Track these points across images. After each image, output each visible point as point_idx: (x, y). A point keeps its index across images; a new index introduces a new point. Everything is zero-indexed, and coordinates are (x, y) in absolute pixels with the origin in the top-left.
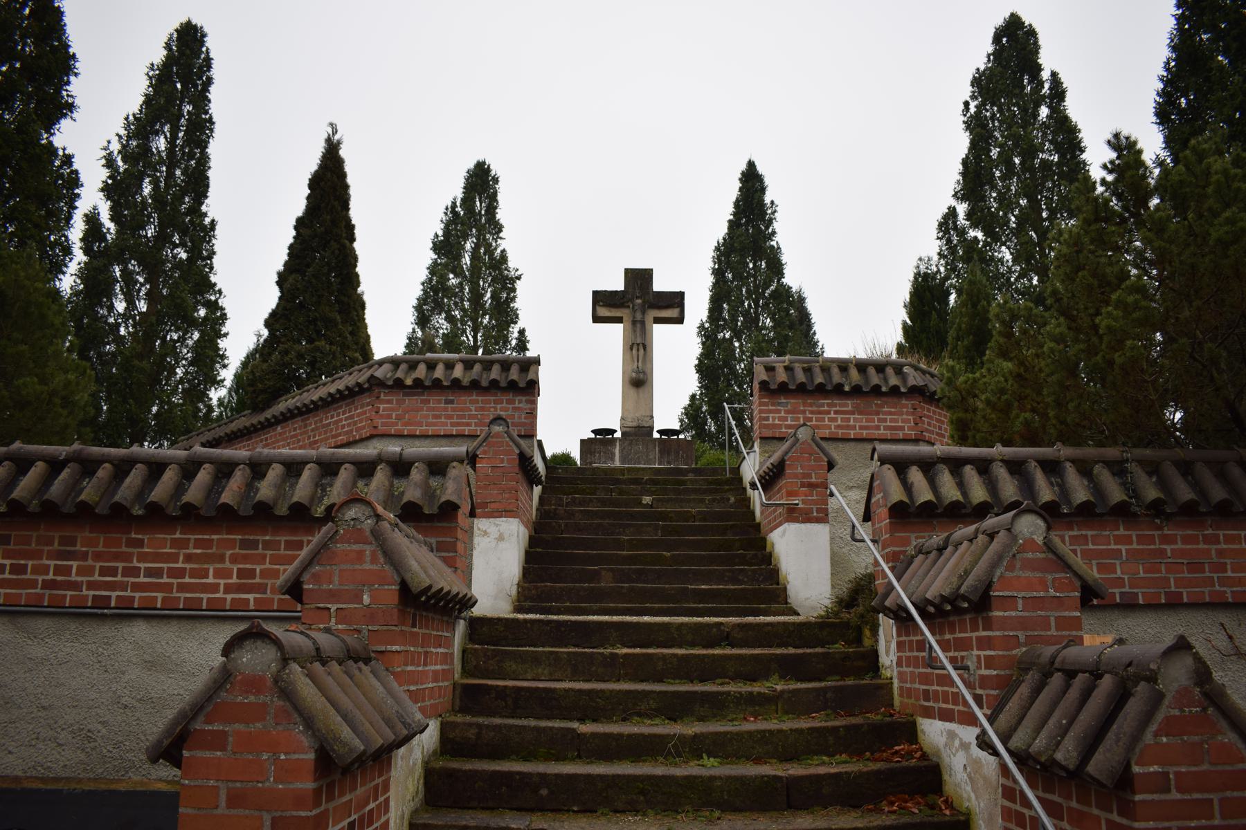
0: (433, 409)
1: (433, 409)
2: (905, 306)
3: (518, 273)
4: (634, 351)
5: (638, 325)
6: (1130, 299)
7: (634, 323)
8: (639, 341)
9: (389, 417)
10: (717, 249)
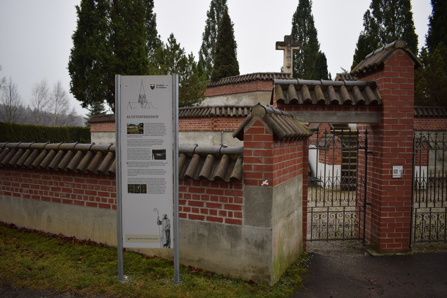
0: (270, 85)
1: (270, 85)
2: (357, 44)
3: (233, 23)
4: (288, 59)
5: (289, 52)
6: (422, 82)
7: (288, 51)
8: (289, 56)
9: (260, 86)
10: (294, 16)
